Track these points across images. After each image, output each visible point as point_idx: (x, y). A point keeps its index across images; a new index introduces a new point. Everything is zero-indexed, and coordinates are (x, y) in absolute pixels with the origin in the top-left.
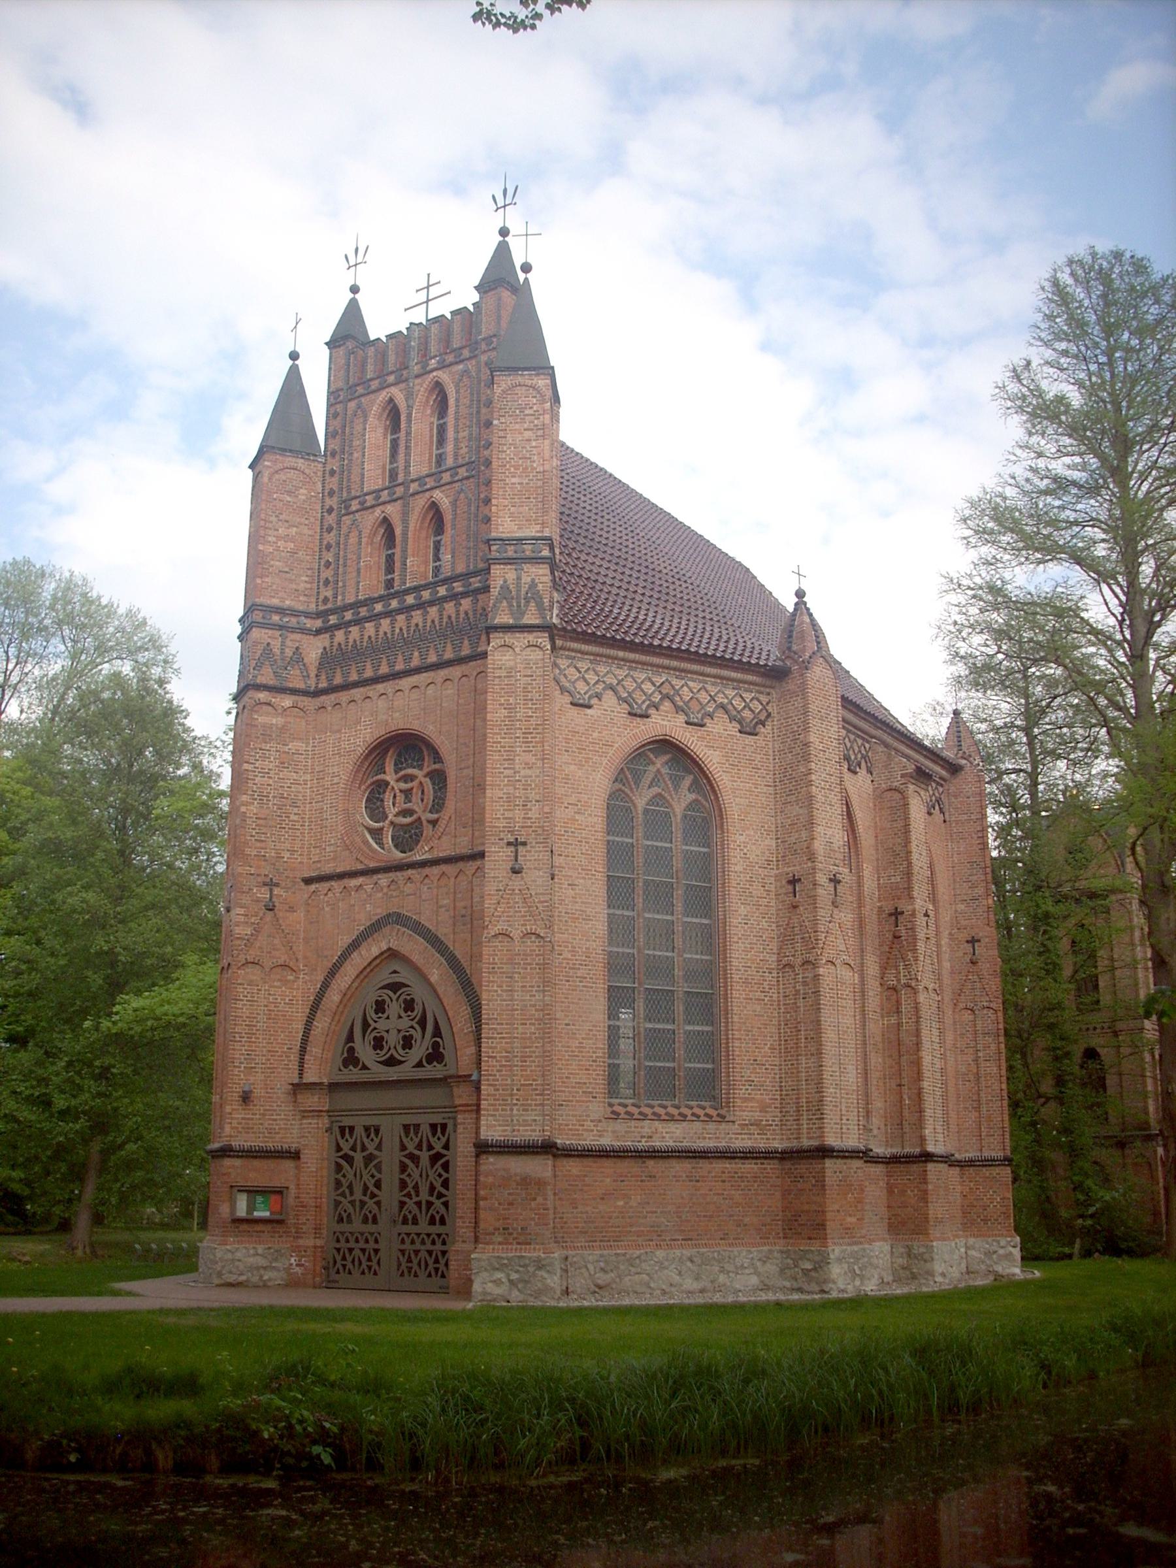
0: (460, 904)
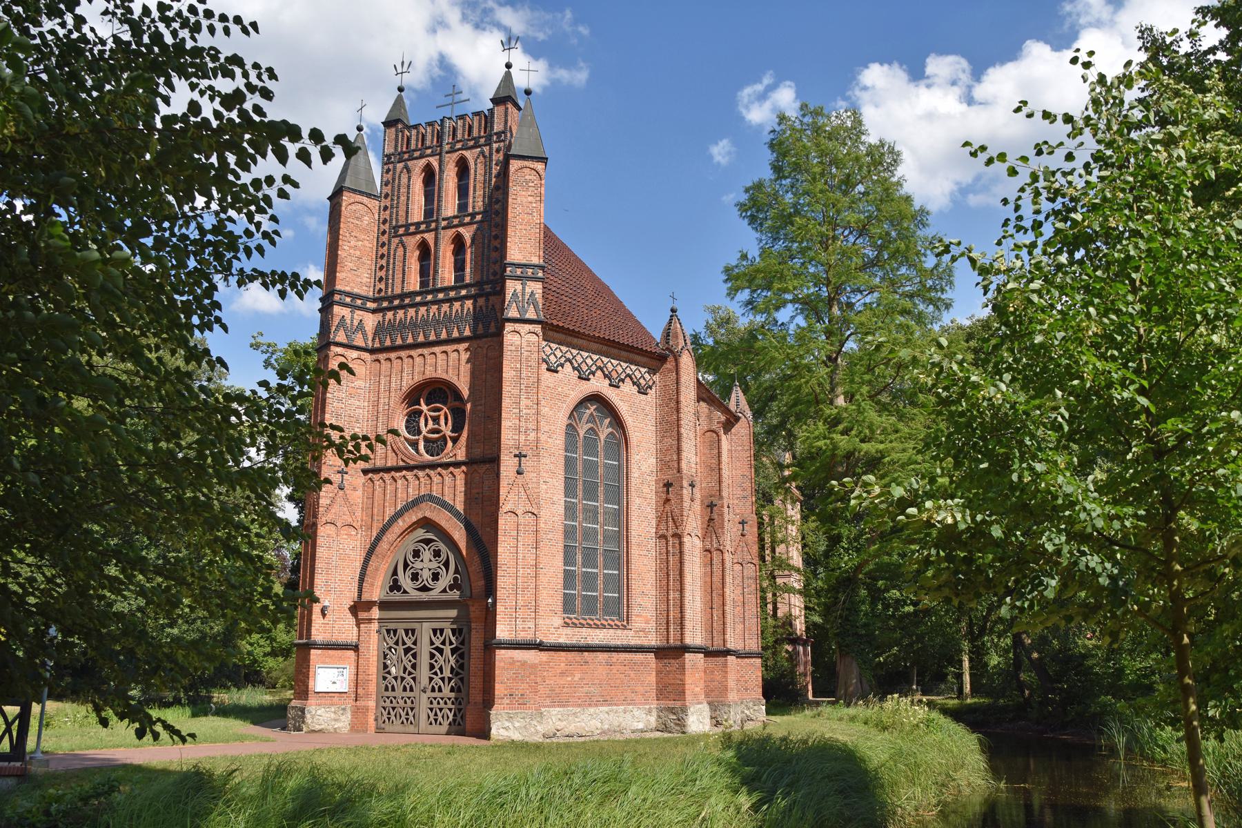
0: (474, 491)
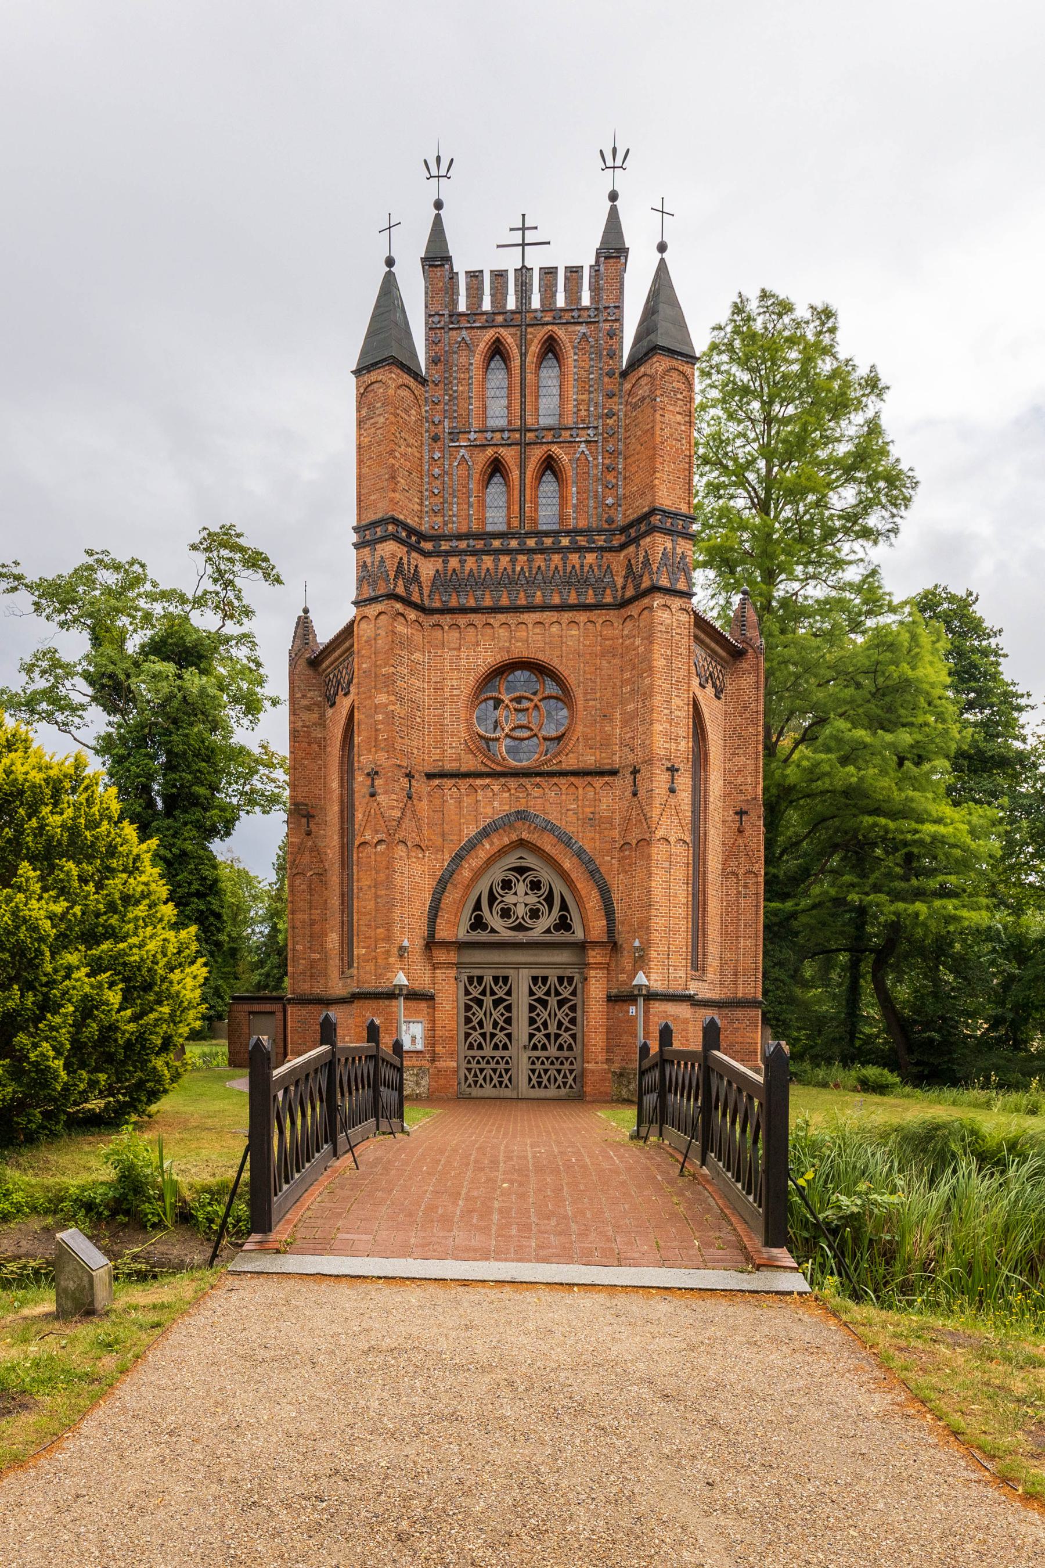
0: (588, 810)
